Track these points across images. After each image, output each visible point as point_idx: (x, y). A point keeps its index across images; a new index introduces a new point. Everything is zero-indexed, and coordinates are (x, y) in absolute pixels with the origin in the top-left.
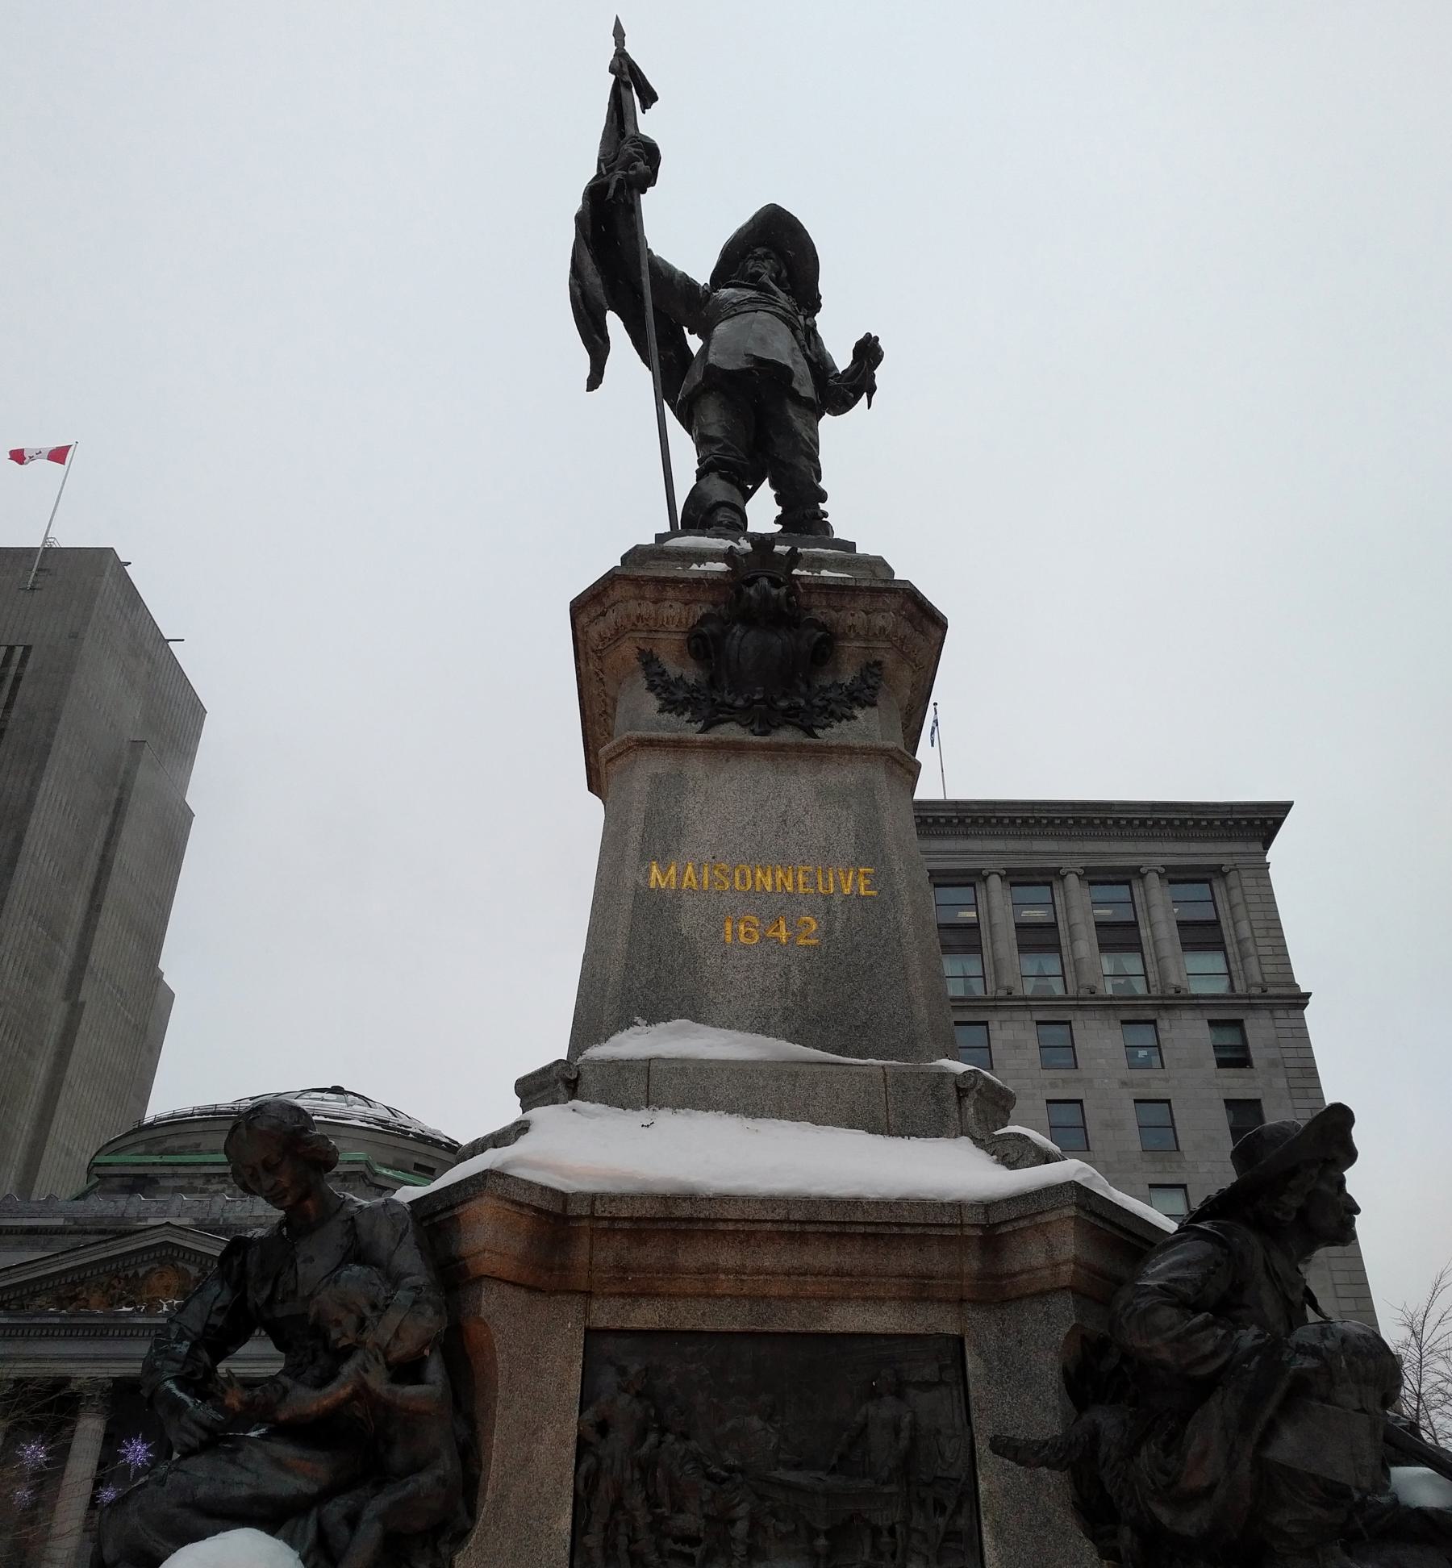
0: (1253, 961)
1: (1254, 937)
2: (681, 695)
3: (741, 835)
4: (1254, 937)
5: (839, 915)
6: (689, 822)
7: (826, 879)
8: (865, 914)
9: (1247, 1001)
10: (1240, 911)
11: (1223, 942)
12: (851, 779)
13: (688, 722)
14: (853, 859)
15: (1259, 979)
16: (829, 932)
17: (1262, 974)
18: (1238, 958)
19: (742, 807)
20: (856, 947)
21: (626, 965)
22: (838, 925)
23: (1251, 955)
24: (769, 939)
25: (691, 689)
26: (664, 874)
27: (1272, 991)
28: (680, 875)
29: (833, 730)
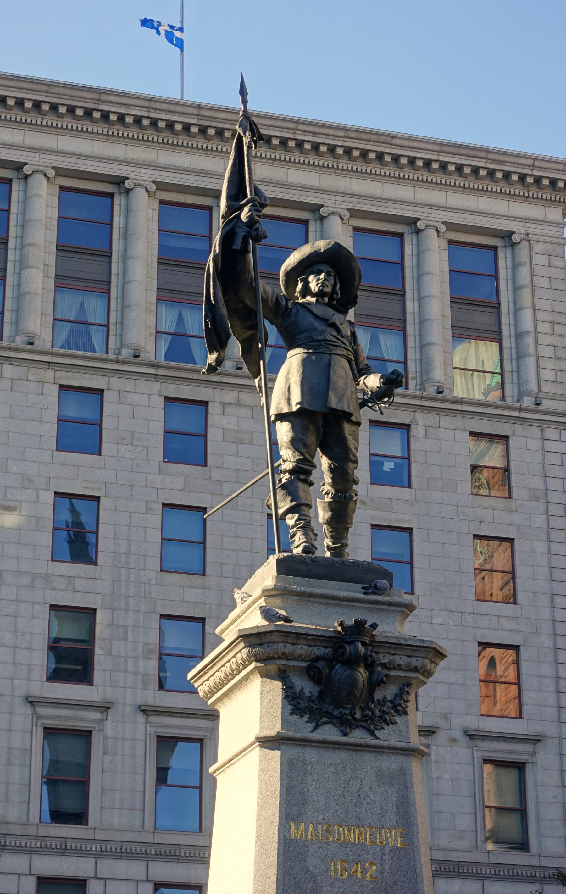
0: (531, 362)
1: (536, 332)
2: (303, 704)
3: (337, 804)
4: (536, 332)
5: (387, 862)
6: (309, 794)
7: (381, 836)
8: (400, 862)
9: (516, 414)
10: (526, 296)
11: (500, 332)
12: (394, 766)
13: (306, 722)
14: (395, 822)
15: (533, 387)
16: (382, 873)
17: (539, 381)
18: (514, 356)
19: (337, 785)
20: (395, 883)
21: (283, 889)
22: (386, 868)
23: (529, 355)
24: (353, 876)
25: (310, 699)
26: (297, 828)
27: (547, 405)
28: (306, 830)
29: (385, 731)
